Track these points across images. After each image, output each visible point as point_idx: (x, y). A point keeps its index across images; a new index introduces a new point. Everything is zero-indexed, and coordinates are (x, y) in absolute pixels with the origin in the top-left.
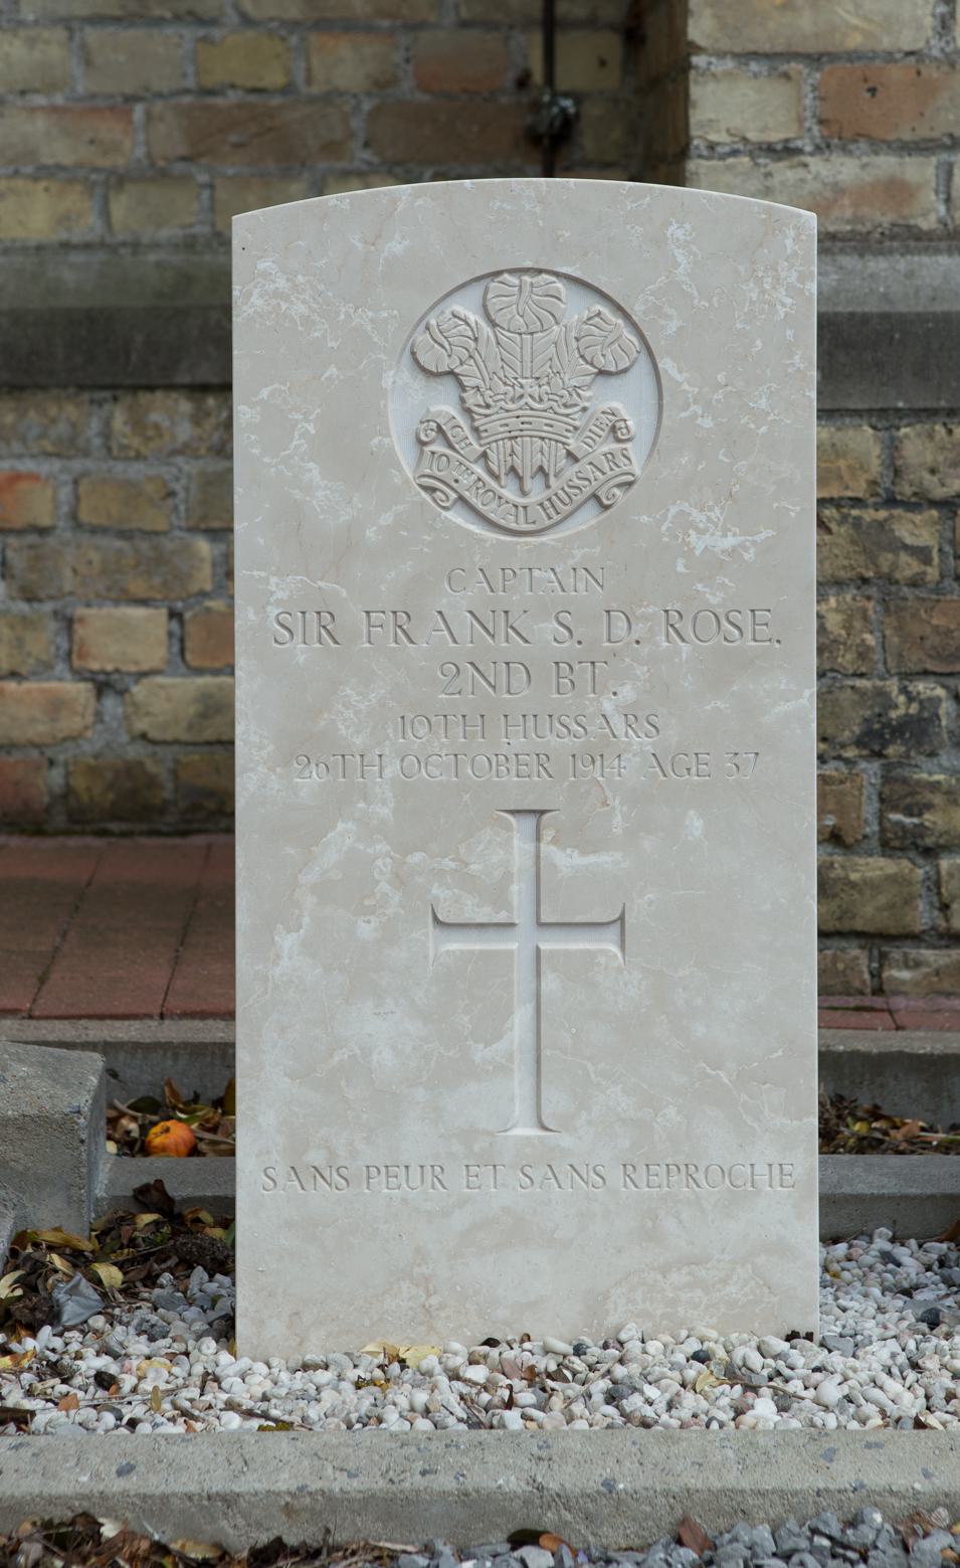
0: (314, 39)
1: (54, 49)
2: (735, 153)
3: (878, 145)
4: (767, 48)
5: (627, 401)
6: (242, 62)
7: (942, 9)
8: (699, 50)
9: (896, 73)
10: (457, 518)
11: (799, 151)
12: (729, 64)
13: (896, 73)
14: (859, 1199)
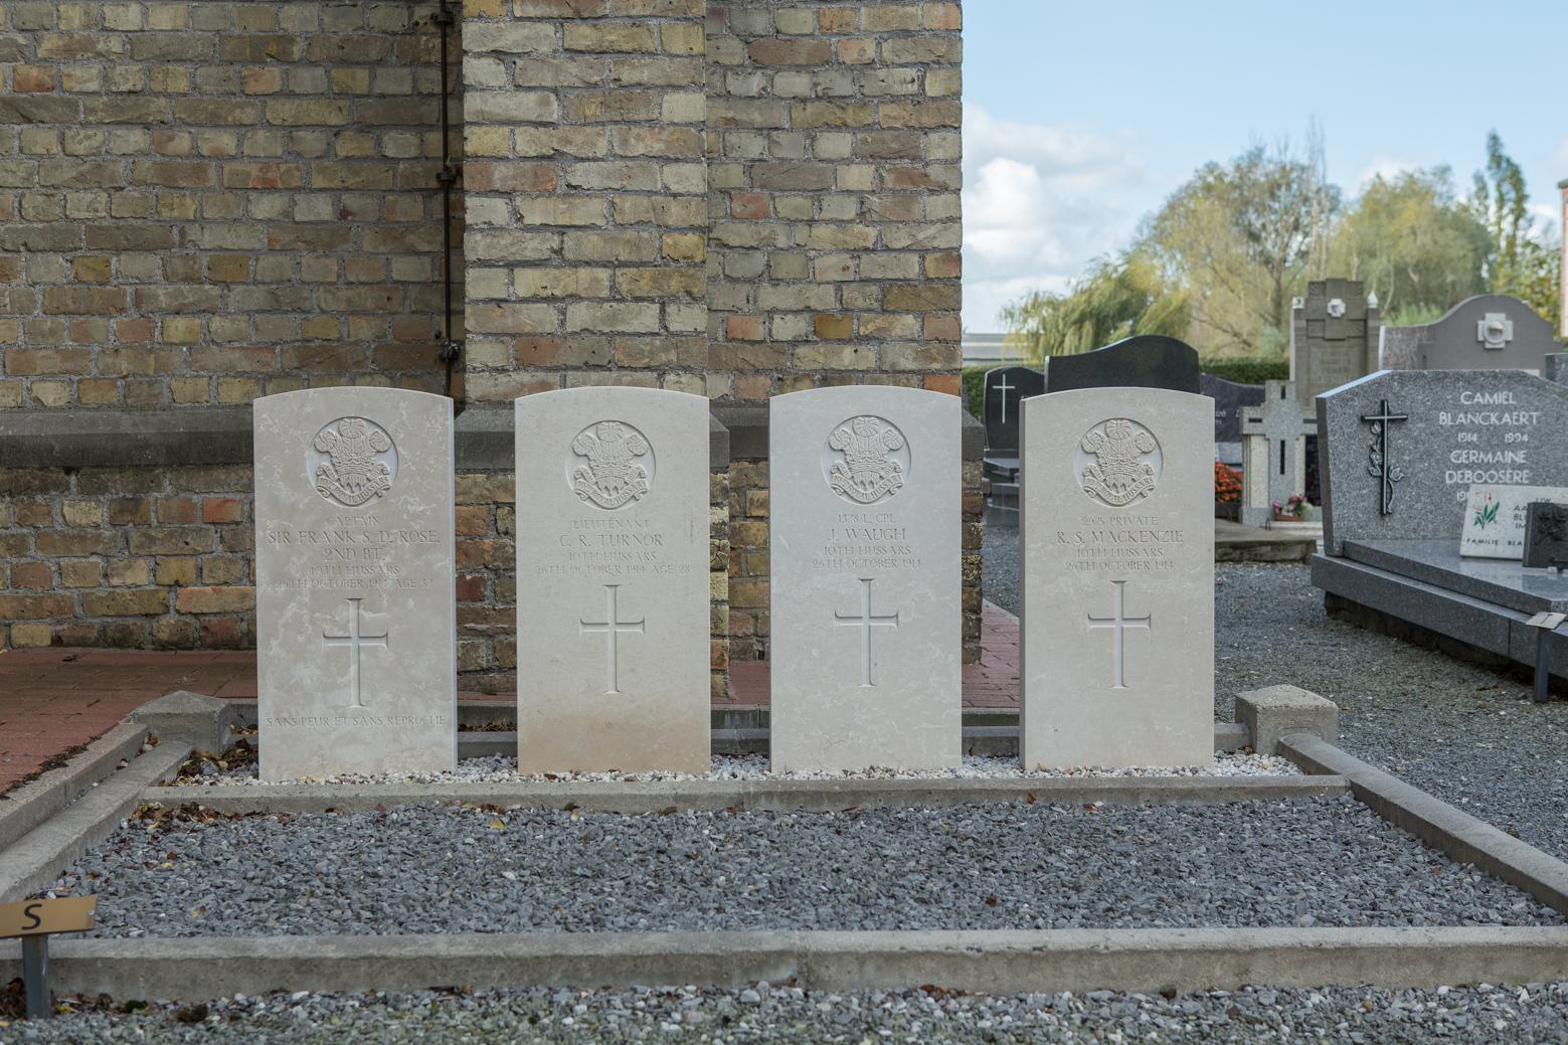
0: (351, 318)
1: (242, 323)
2: (483, 371)
3: (538, 368)
5: (386, 462)
6: (322, 328)
7: (561, 317)
8: (469, 332)
9: (544, 341)
10: (330, 500)
12: (481, 337)
13: (544, 341)
14: (491, 743)
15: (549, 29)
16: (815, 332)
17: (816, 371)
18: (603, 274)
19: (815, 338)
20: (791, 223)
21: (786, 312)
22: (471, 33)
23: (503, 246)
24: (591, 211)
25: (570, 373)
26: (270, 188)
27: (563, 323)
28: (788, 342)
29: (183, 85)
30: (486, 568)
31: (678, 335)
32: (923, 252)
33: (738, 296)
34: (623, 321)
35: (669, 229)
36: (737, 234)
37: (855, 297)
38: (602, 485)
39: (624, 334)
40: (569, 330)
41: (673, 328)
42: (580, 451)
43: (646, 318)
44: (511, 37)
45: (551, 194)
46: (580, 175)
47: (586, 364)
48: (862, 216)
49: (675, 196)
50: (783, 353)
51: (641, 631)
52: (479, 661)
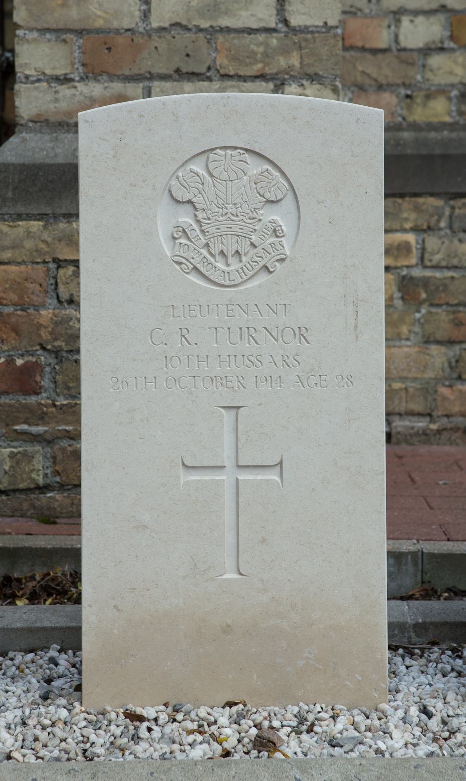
2: (39, 80)
3: (113, 77)
4: (54, 26)
7: (144, 7)
9: (121, 40)
11: (72, 80)
12: (35, 34)
13: (121, 40)
14: (44, 629)
16: (452, 37)
17: (453, 86)
19: (452, 45)
21: (416, 13)
25: (156, 83)
27: (146, 15)
28: (420, 50)
30: (43, 348)
31: (301, 31)
34: (227, 12)
38: (216, 248)
39: (229, 30)
40: (155, 24)
41: (295, 20)
42: (180, 195)
47: (178, 71)
50: (412, 64)
51: (276, 478)
52: (33, 475)
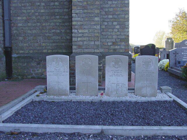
15: (82, 10)
18: (88, 38)
20: (110, 32)
21: (110, 42)
22: (73, 11)
23: (76, 35)
24: (86, 31)
26: (54, 29)
29: (44, 18)
32: (125, 35)
33: (104, 40)
35: (95, 33)
36: (104, 33)
37: (118, 40)
43: (93, 43)
44: (77, 11)
45: (82, 29)
46: (85, 27)
48: (118, 31)
49: (96, 29)
